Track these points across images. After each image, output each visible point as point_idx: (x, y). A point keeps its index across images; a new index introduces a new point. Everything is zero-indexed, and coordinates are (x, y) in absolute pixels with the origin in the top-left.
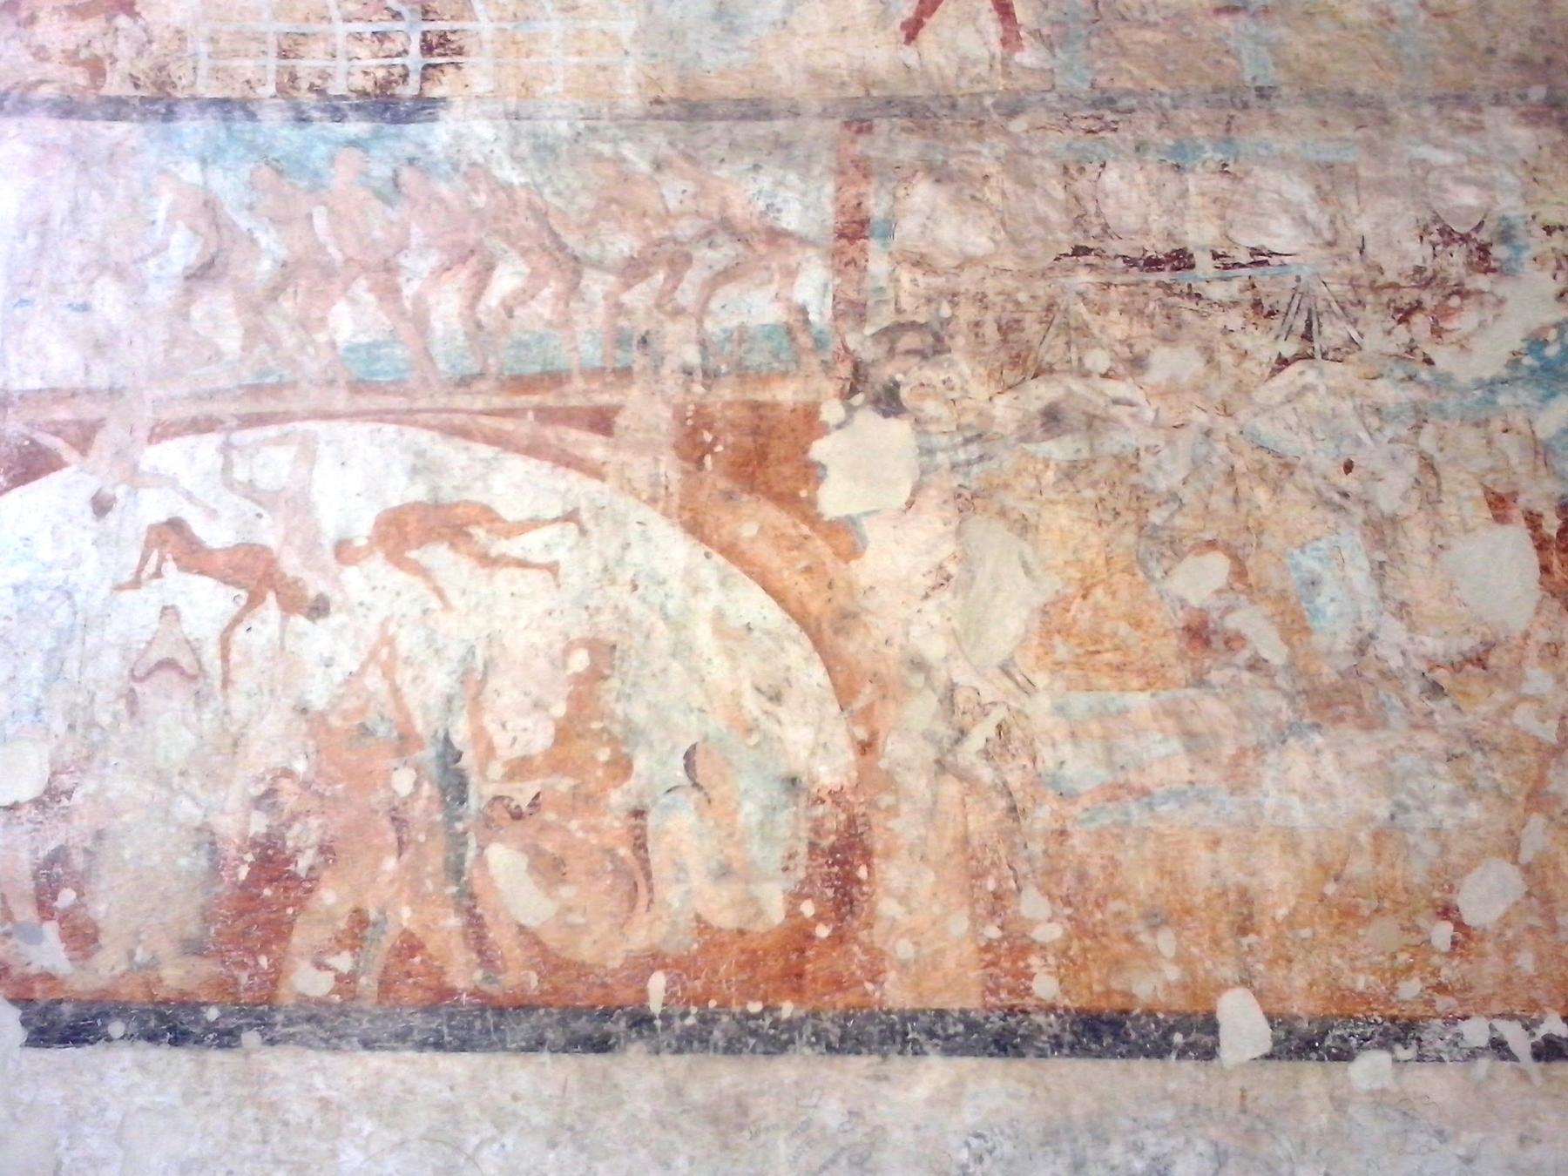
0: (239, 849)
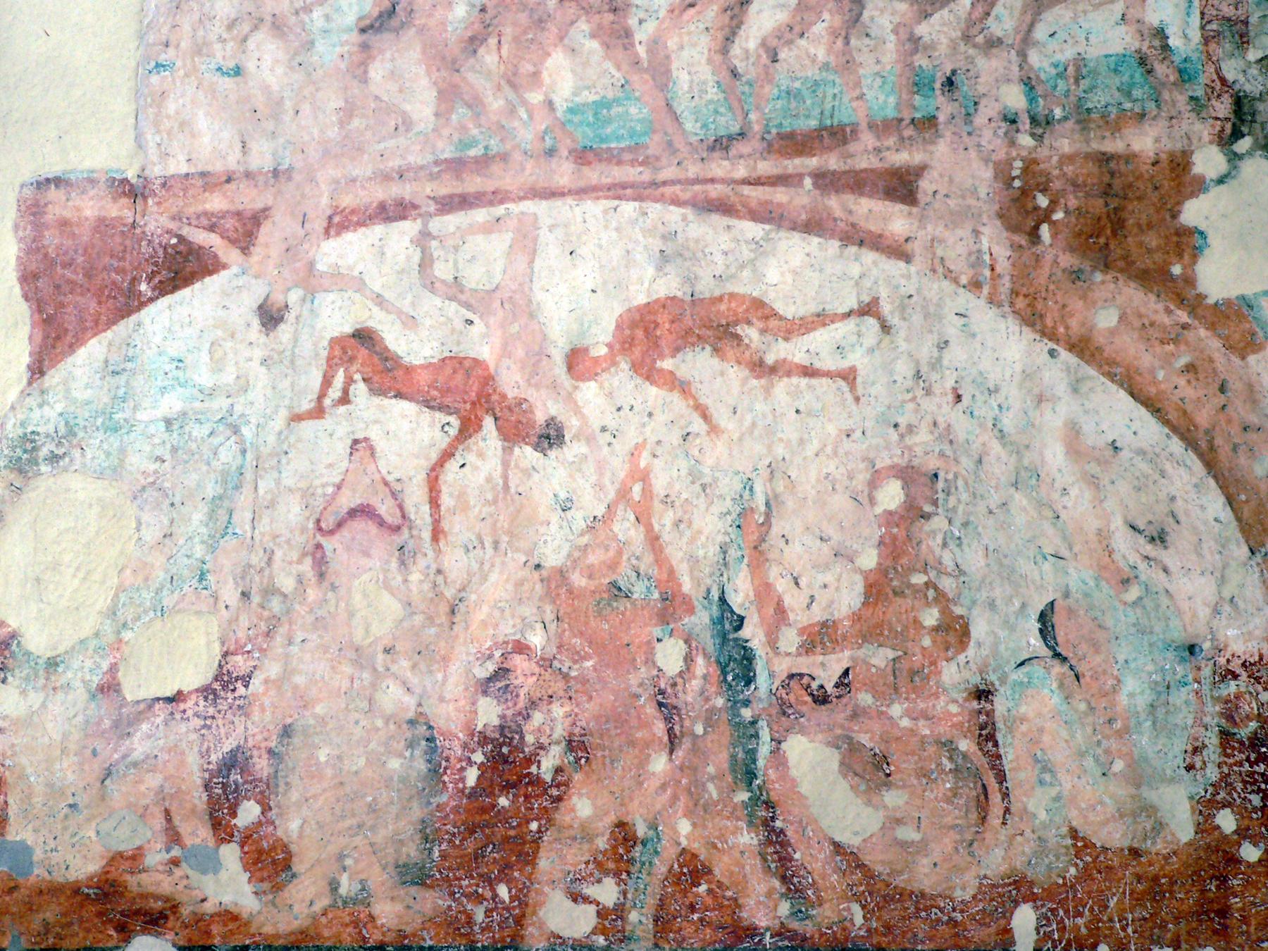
0: (465, 746)
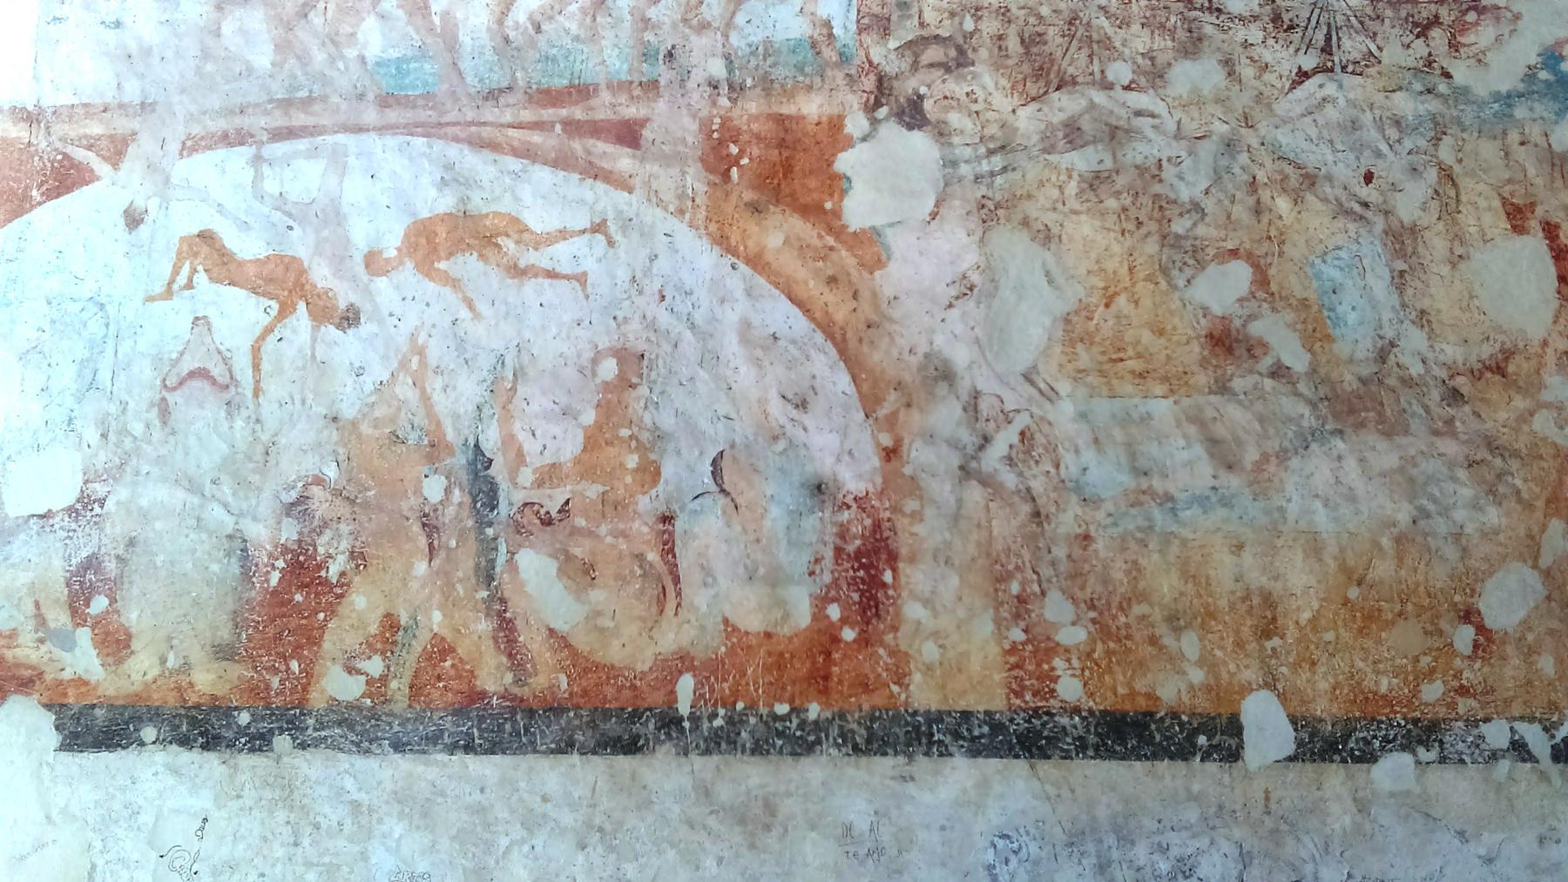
0: (270, 556)
